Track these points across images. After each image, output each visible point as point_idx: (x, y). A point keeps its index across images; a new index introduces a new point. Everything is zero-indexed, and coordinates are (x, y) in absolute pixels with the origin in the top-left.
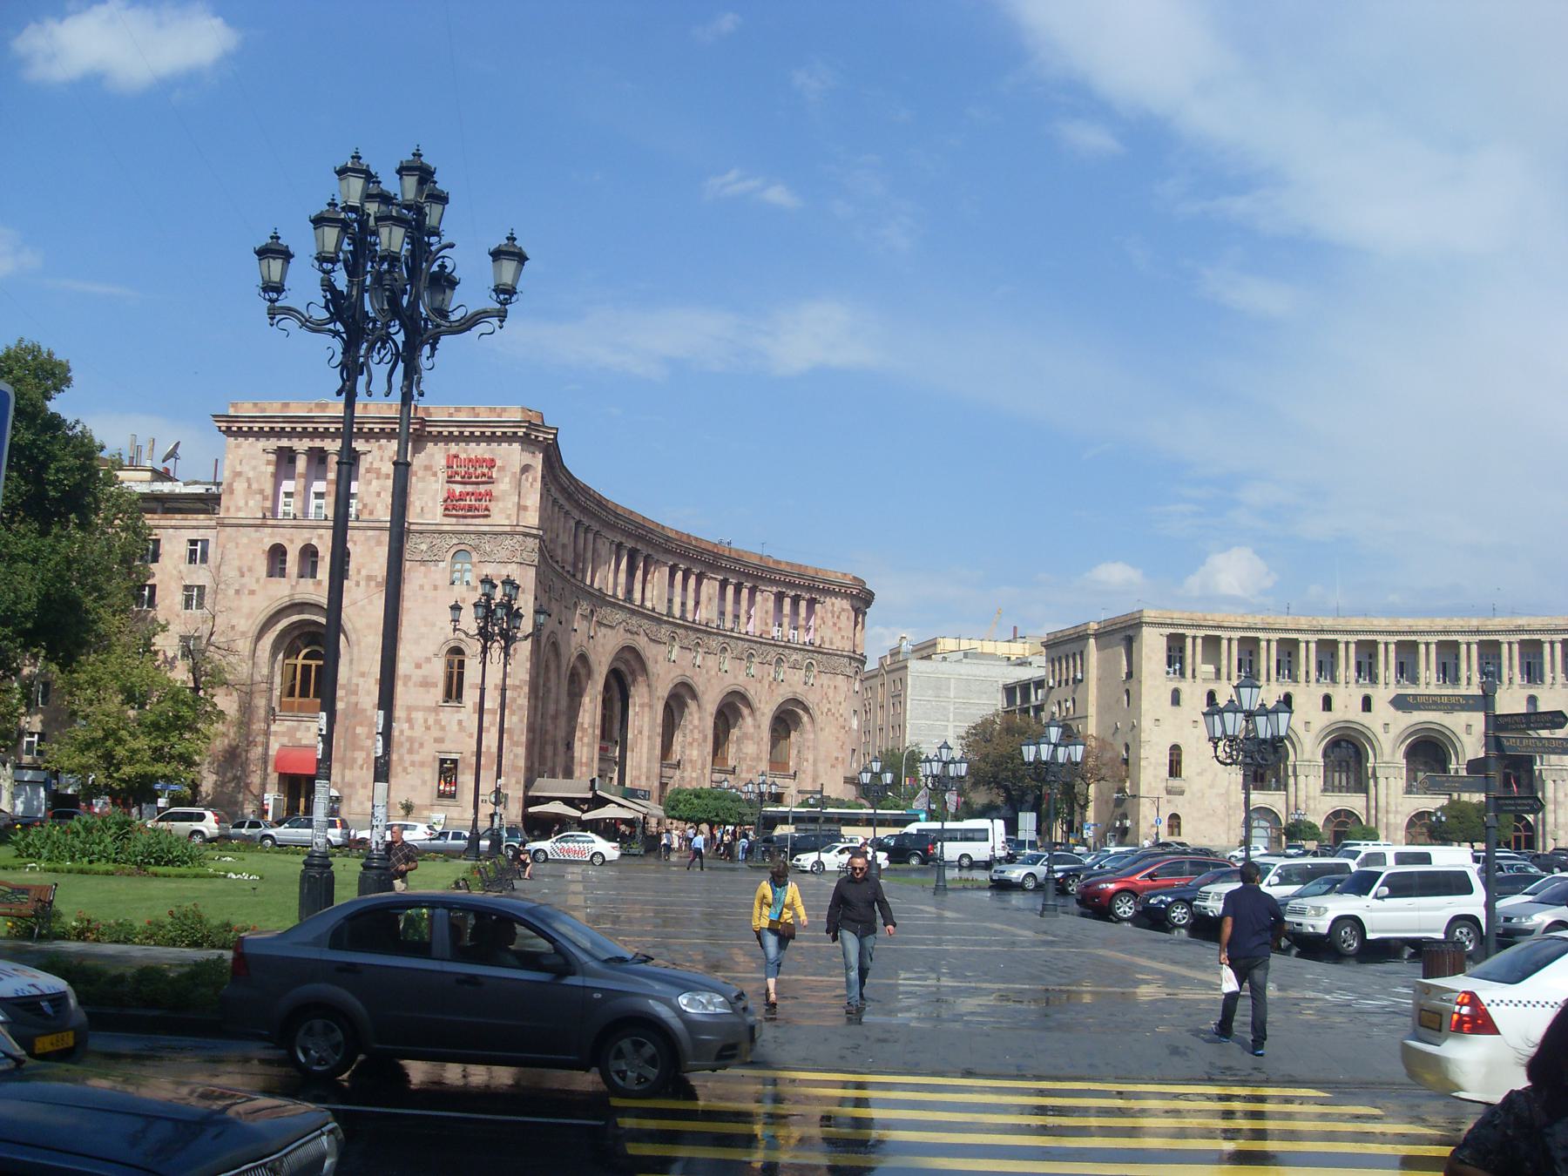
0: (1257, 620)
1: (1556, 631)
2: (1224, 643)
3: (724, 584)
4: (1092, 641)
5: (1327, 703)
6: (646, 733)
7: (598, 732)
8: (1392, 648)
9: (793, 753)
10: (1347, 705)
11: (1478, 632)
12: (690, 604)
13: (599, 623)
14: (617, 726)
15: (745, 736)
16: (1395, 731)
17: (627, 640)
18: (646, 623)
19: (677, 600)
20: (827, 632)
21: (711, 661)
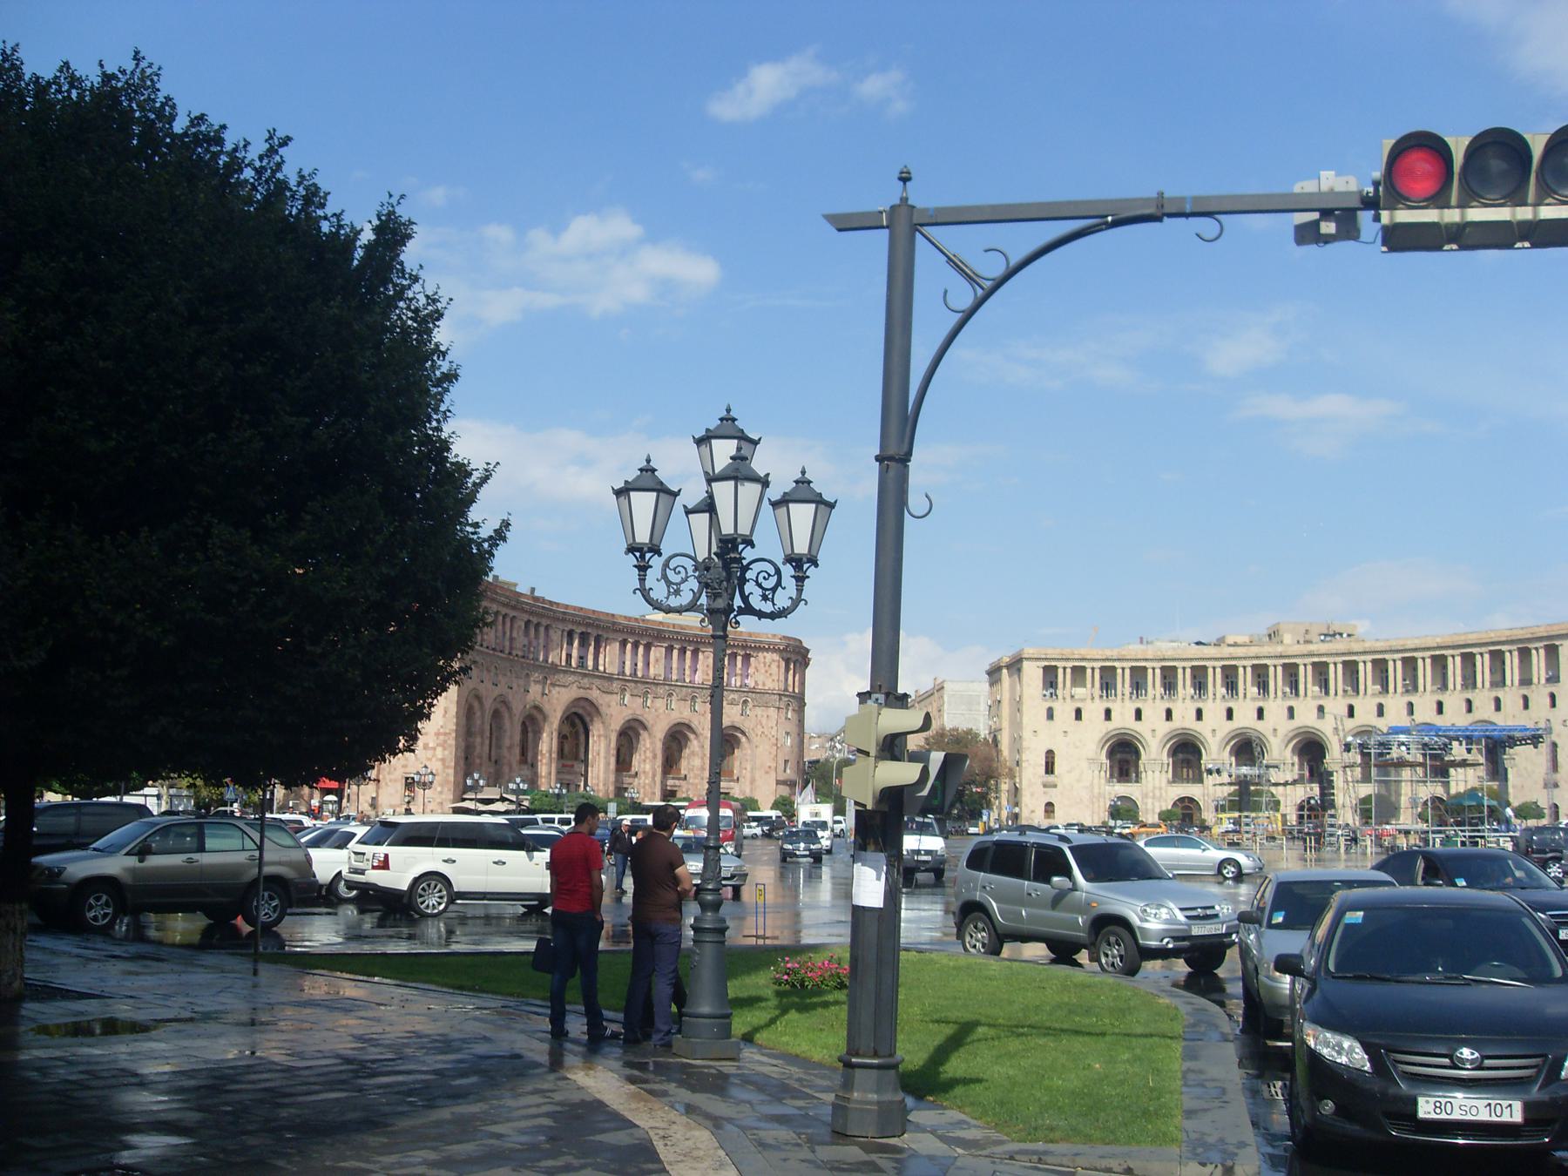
0: (1114, 653)
1: (1337, 654)
2: (1089, 671)
3: (670, 649)
4: (1005, 671)
5: (1169, 714)
6: (602, 754)
7: (554, 755)
8: (1218, 671)
9: (737, 764)
10: (1184, 718)
11: (1281, 657)
12: (640, 665)
13: (553, 685)
14: (582, 750)
15: (693, 753)
16: (1220, 735)
17: (582, 693)
18: (597, 682)
19: (628, 663)
20: (760, 678)
21: (660, 703)
